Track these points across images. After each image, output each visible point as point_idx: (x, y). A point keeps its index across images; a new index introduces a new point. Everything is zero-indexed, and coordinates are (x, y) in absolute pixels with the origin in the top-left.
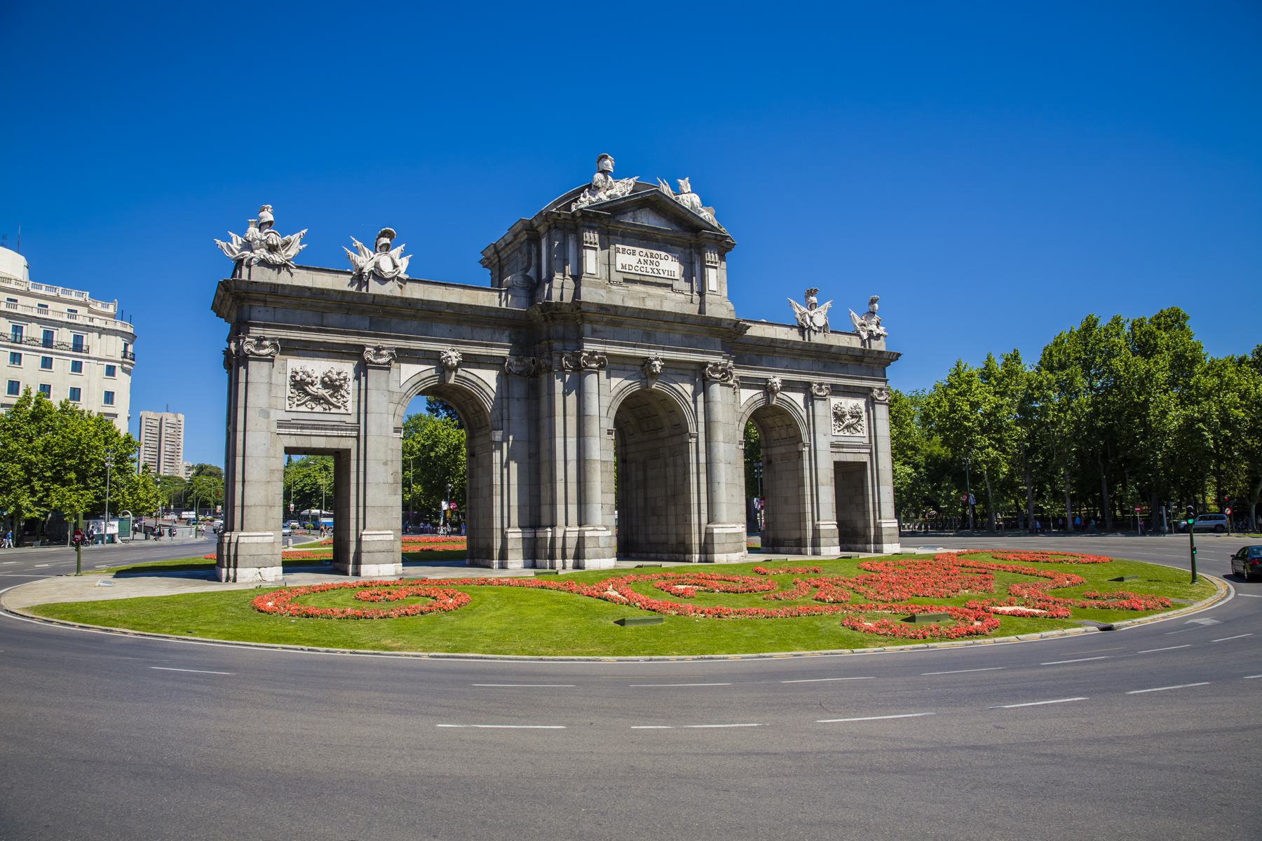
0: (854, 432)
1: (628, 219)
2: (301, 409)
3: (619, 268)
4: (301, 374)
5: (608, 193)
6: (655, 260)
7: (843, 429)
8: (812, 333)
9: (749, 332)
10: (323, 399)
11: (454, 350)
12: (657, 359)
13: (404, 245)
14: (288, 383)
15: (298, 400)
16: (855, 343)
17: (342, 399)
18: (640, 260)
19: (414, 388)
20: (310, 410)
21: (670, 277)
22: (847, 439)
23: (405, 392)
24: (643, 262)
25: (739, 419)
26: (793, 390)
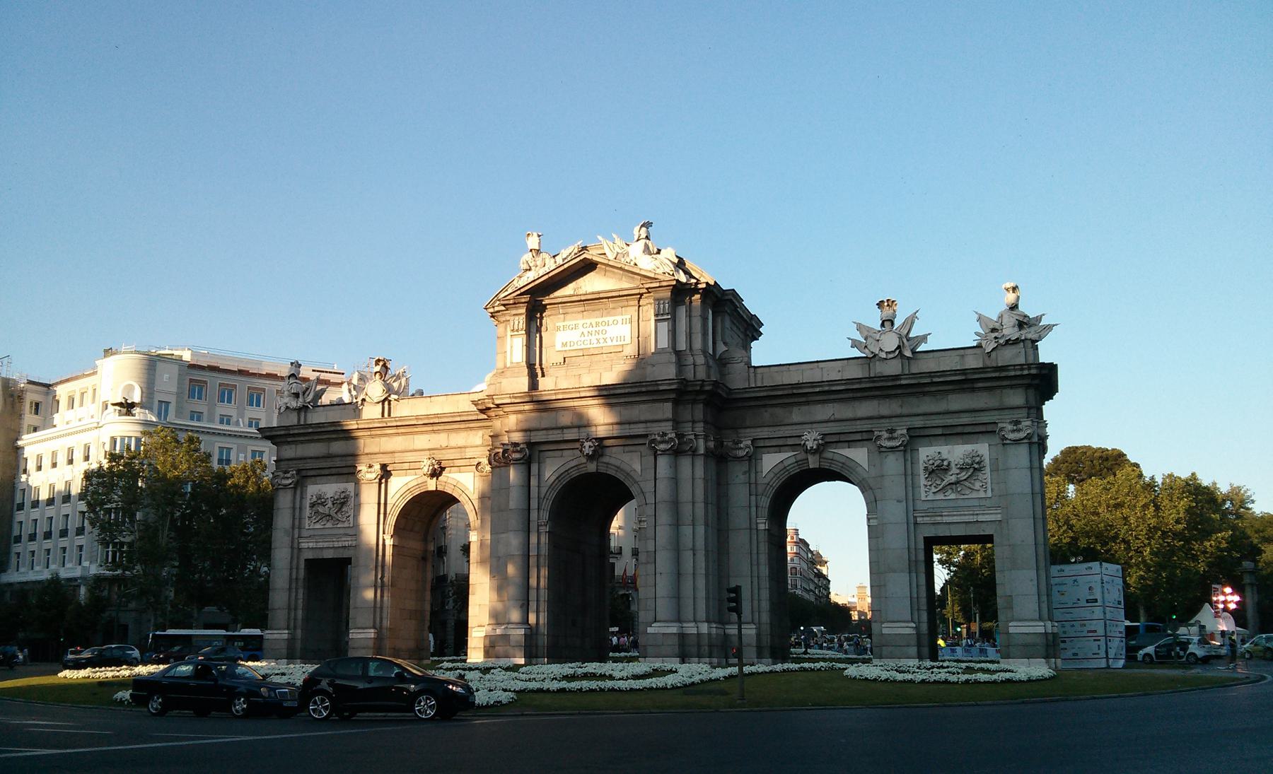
2: (318, 526)
3: (559, 347)
4: (314, 497)
6: (601, 328)
10: (329, 515)
12: (587, 440)
14: (308, 505)
19: (402, 498)
20: (322, 527)
21: (619, 343)
22: (951, 504)
24: (586, 333)
26: (850, 443)
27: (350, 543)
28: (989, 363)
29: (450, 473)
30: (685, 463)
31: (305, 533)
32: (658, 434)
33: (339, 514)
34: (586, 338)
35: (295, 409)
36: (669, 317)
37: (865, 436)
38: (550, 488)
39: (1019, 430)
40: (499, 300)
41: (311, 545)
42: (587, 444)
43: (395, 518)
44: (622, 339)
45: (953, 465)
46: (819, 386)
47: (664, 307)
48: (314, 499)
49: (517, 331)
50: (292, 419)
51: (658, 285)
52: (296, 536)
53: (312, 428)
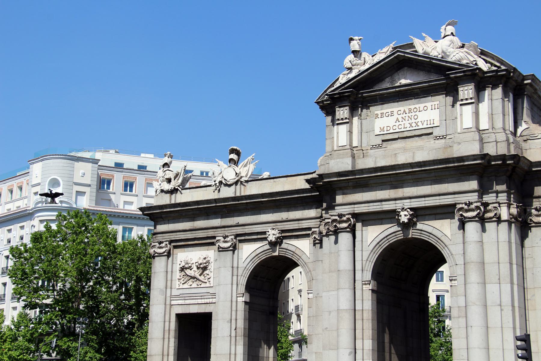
1: (386, 84)
4: (183, 262)
6: (413, 114)
11: (273, 229)
12: (403, 209)
13: (253, 155)
17: (206, 278)
18: (397, 118)
20: (189, 287)
21: (429, 126)
23: (245, 266)
30: (490, 226)
32: (466, 204)
33: (202, 276)
34: (401, 123)
35: (167, 192)
36: (473, 101)
38: (372, 251)
40: (327, 95)
42: (402, 213)
43: (247, 279)
44: (432, 123)
47: (468, 93)
48: (183, 264)
49: (342, 119)
50: (166, 200)
52: (168, 294)
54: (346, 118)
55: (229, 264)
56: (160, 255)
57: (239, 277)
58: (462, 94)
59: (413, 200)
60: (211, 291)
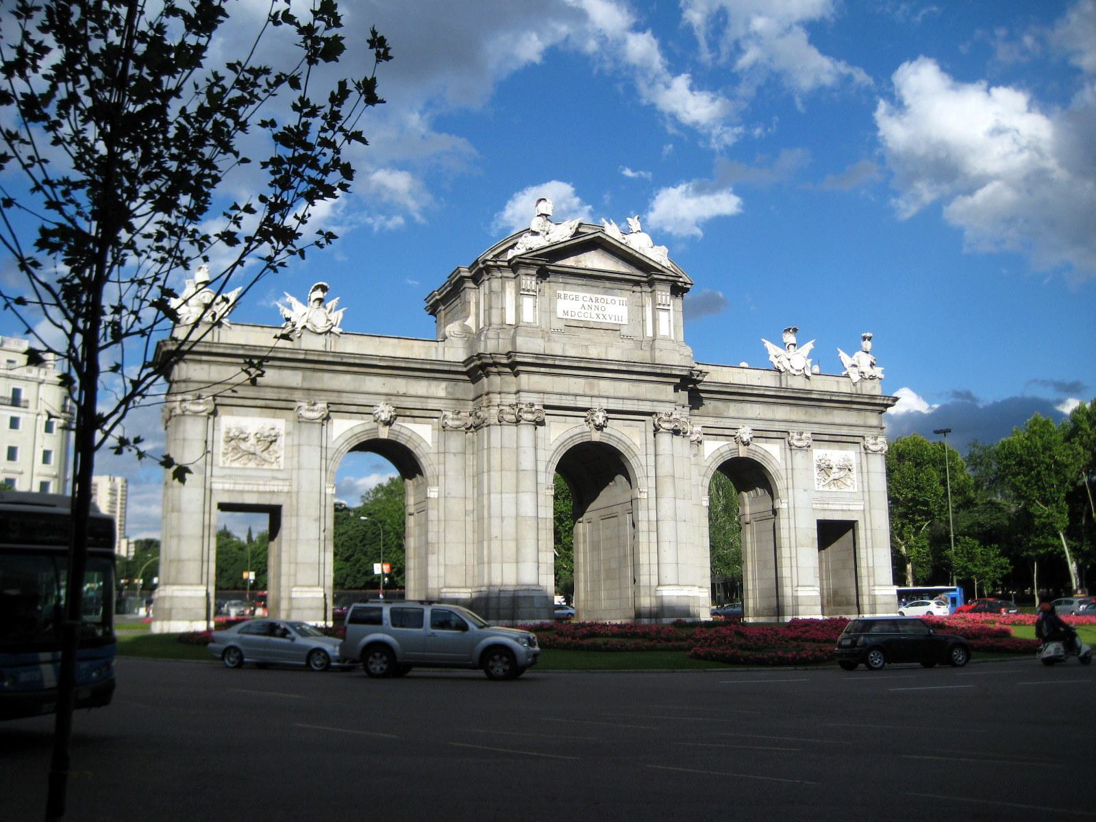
0: (843, 487)
3: (560, 314)
4: (234, 430)
5: (547, 237)
6: (600, 305)
7: (829, 484)
8: (789, 377)
9: (705, 379)
10: (254, 454)
13: (338, 298)
15: (232, 457)
16: (844, 387)
20: (242, 466)
21: (617, 322)
25: (703, 473)
27: (280, 488)
28: (854, 391)
29: (404, 422)
30: (677, 439)
31: (216, 471)
33: (265, 452)
37: (779, 435)
39: (876, 444)
41: (227, 486)
45: (834, 466)
46: (757, 389)
49: (528, 291)
51: (664, 277)
53: (245, 349)
54: (533, 291)
55: (316, 442)
56: (196, 414)
57: (328, 462)
58: (659, 297)
59: (610, 400)
60: (280, 475)
